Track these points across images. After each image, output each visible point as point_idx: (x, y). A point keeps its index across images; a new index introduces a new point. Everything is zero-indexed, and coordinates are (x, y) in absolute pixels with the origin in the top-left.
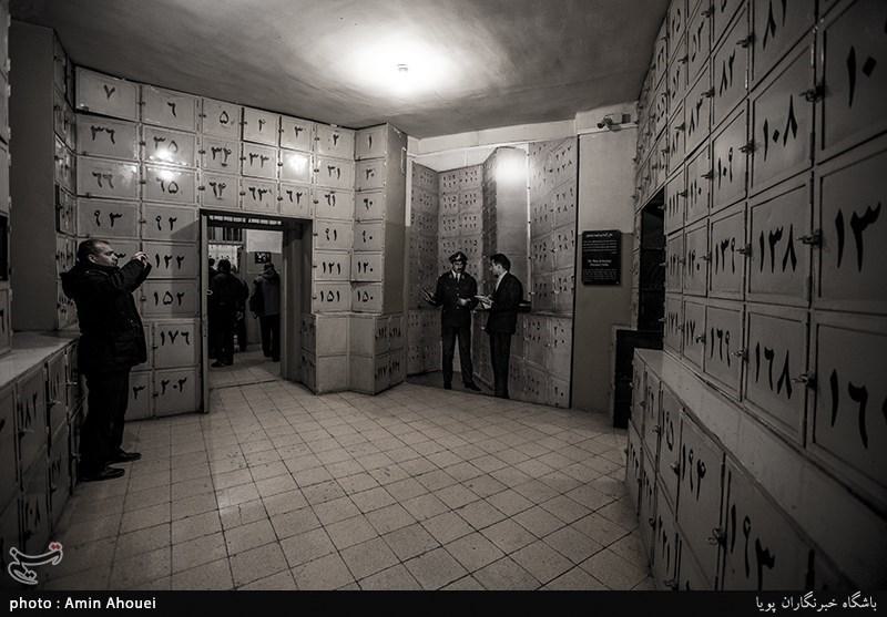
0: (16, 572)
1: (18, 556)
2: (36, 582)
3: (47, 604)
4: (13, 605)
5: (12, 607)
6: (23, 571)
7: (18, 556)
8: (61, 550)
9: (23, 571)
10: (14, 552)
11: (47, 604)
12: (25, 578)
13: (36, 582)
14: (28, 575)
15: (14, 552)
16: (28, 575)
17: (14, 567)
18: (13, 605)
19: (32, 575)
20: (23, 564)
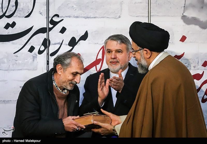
0: (3, 133)
1: (4, 130)
2: (8, 136)
3: (10, 141)
4: (3, 141)
5: (3, 142)
6: (5, 133)
7: (4, 130)
8: (14, 128)
9: (5, 133)
10: (3, 129)
11: (10, 141)
12: (6, 135)
13: (8, 136)
14: (6, 134)
15: (3, 129)
16: (6, 134)
17: (3, 132)
18: (3, 141)
19: (7, 134)
20: (5, 132)
